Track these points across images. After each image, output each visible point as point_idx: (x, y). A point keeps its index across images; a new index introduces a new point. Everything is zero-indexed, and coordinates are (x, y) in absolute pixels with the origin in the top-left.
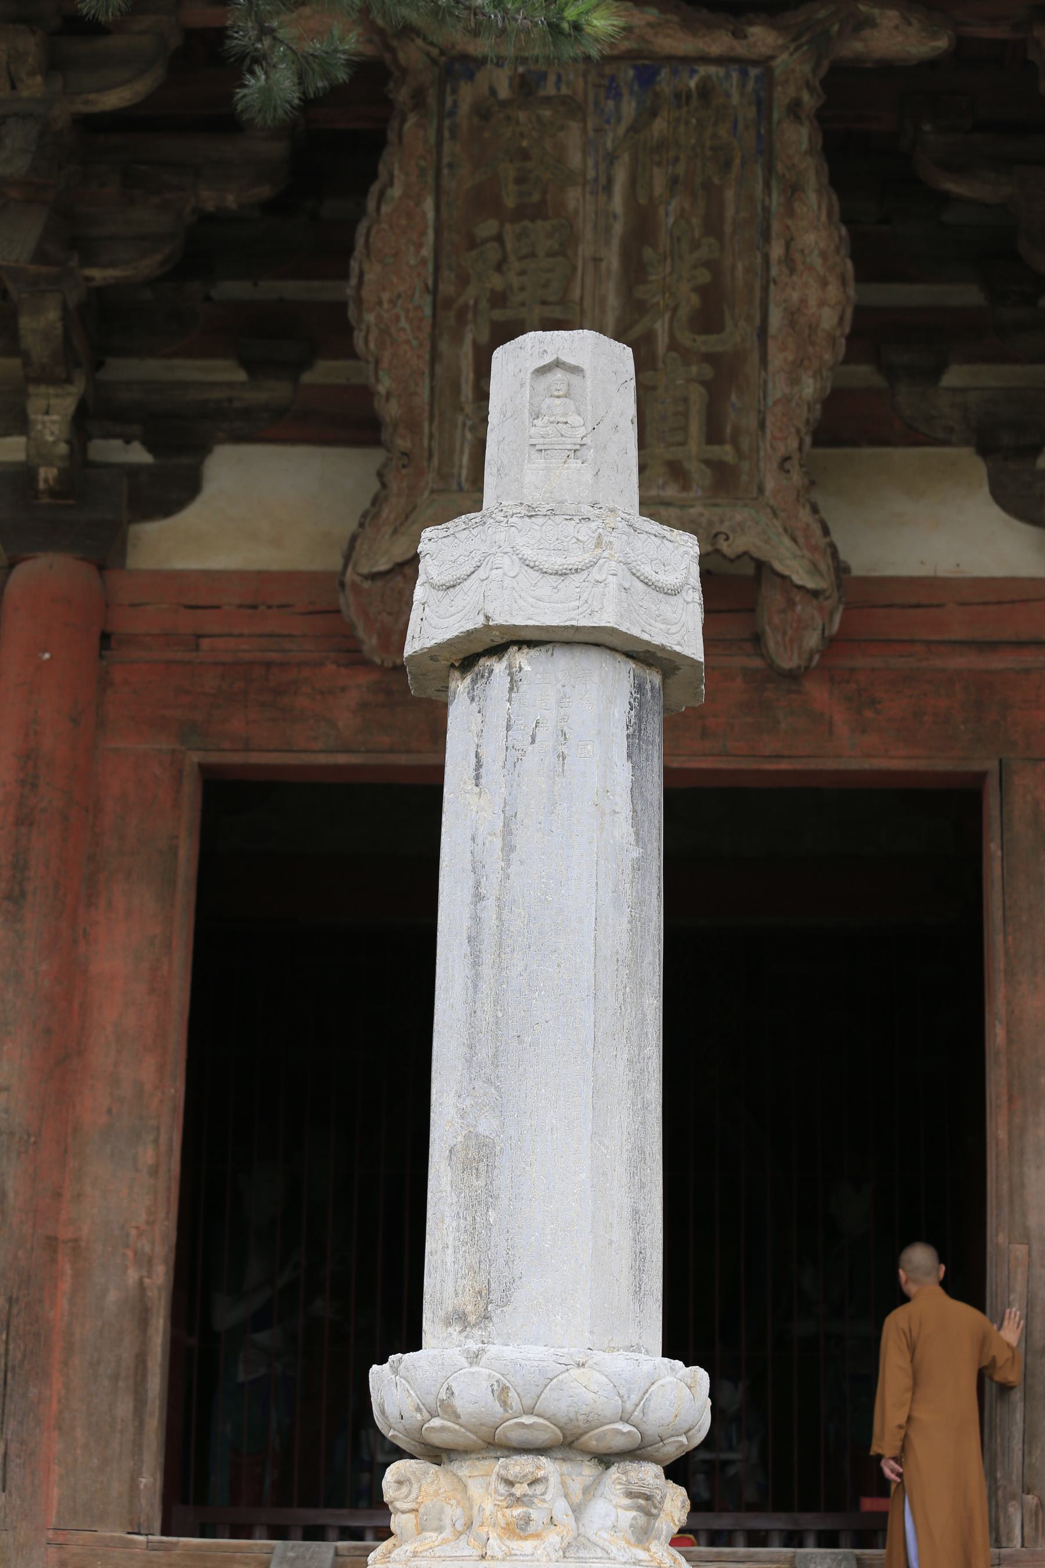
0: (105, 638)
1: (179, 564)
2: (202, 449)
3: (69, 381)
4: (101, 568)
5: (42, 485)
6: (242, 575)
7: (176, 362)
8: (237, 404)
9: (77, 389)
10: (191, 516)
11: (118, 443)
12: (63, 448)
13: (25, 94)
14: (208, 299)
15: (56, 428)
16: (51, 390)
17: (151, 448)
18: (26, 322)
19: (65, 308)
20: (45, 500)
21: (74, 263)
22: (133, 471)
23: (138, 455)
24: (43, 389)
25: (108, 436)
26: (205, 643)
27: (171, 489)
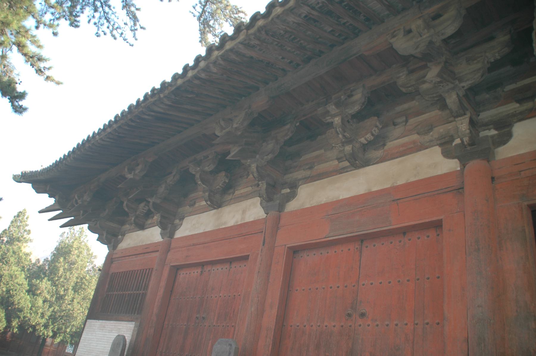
0: (493, 179)
1: (510, 155)
2: (510, 125)
3: (465, 114)
4: (488, 161)
5: (466, 143)
6: (529, 153)
7: (499, 108)
8: (517, 112)
9: (468, 115)
10: (511, 143)
11: (487, 131)
12: (468, 131)
13: (424, 37)
14: (503, 91)
15: (465, 127)
16: (461, 118)
17: (496, 129)
18: (448, 101)
19: (458, 95)
20: (469, 148)
21: (457, 82)
22: (492, 137)
23: (493, 132)
24: (459, 118)
25: (485, 130)
26: (522, 173)
27: (505, 137)
